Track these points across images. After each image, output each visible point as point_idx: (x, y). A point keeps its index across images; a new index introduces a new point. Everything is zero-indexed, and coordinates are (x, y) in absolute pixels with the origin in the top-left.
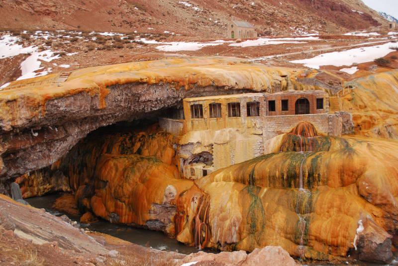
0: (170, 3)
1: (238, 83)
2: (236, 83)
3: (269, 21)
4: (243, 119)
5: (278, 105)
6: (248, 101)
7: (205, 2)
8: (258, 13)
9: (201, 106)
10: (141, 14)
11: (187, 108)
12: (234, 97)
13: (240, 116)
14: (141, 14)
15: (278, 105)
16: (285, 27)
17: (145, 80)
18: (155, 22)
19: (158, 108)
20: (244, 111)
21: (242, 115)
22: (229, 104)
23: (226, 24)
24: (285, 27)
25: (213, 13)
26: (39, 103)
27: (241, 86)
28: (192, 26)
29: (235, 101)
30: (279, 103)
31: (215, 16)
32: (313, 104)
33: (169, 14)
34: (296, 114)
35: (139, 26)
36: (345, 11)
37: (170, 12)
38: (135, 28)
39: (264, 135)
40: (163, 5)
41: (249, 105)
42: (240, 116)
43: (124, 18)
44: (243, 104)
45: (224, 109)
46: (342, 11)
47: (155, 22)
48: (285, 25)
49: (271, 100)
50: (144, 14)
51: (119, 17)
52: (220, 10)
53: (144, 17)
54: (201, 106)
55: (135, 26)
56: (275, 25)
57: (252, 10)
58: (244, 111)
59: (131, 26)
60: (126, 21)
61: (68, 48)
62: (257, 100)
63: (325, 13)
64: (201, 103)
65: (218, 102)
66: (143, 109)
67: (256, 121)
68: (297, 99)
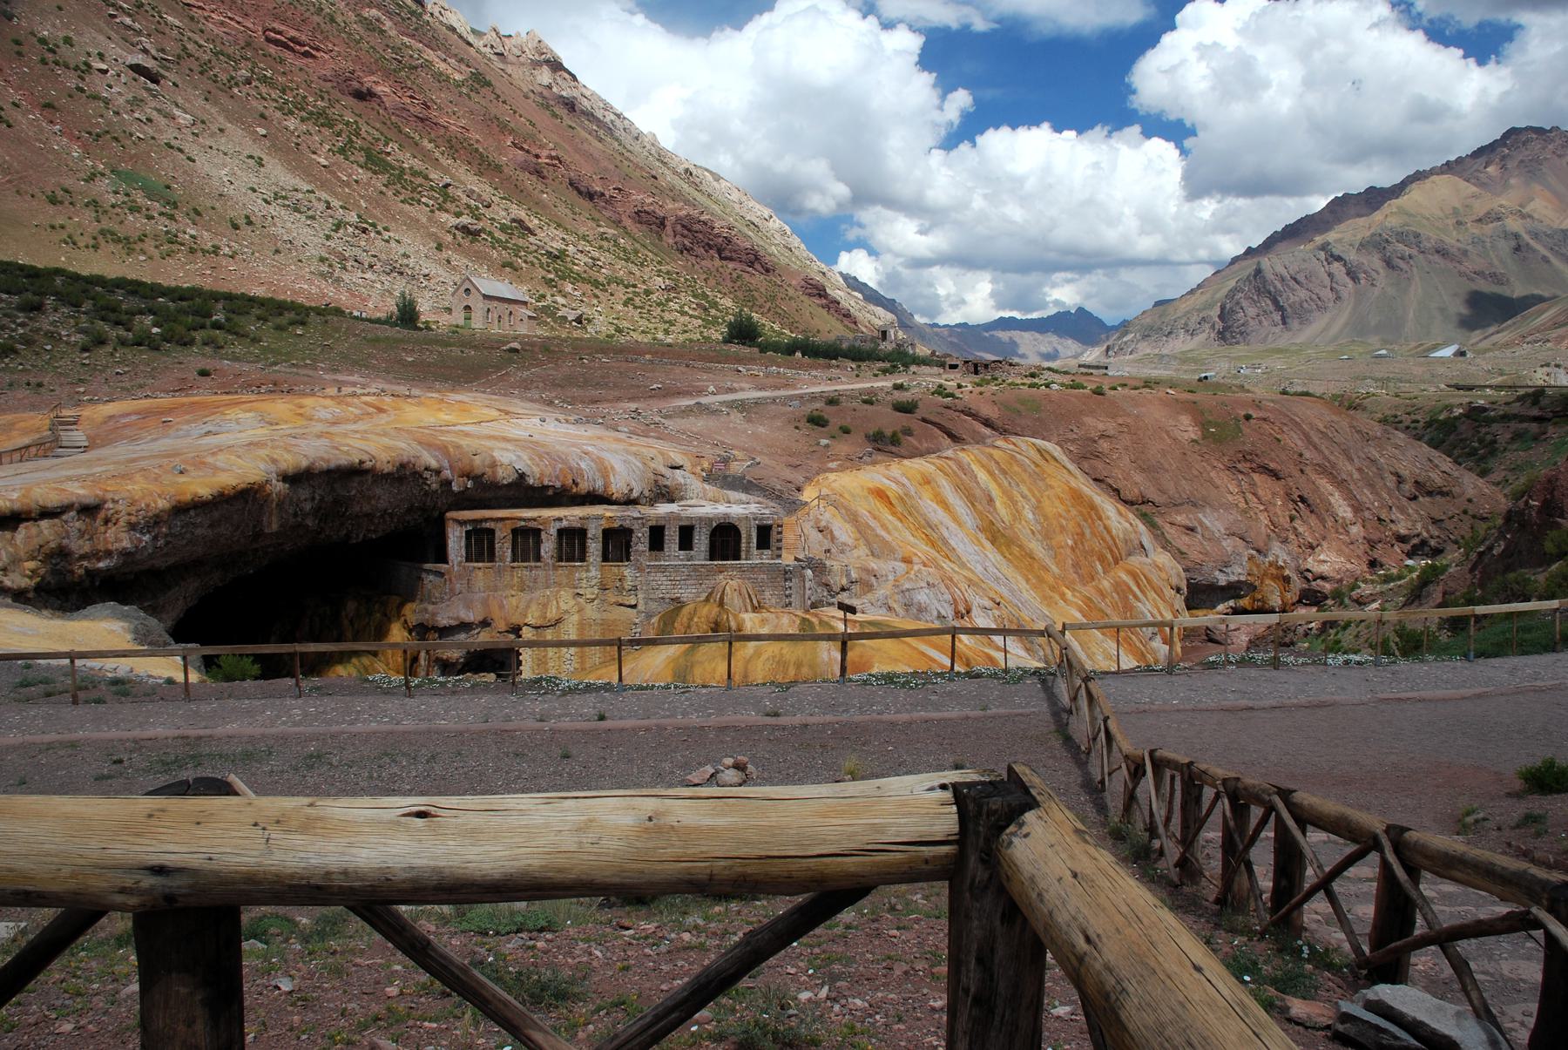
0: (254, 190)
3: (552, 276)
4: (592, 570)
5: (672, 537)
6: (605, 524)
7: (362, 197)
8: (519, 248)
9: (492, 532)
10: (161, 214)
11: (455, 540)
12: (572, 515)
13: (583, 559)
14: (161, 214)
15: (672, 537)
16: (597, 297)
18: (209, 246)
19: (380, 534)
20: (594, 548)
23: (427, 272)
24: (597, 297)
25: (386, 235)
27: (584, 487)
28: (325, 268)
31: (393, 244)
32: (749, 537)
33: (250, 223)
34: (711, 559)
35: (156, 253)
36: (757, 266)
37: (253, 219)
38: (142, 258)
40: (232, 192)
41: (608, 534)
42: (583, 559)
43: (106, 224)
44: (594, 531)
46: (751, 264)
47: (209, 246)
48: (597, 291)
49: (654, 523)
50: (172, 217)
51: (89, 214)
52: (409, 227)
53: (173, 227)
54: (492, 532)
55: (143, 252)
56: (569, 288)
57: (503, 237)
58: (594, 548)
59: (130, 252)
60: (113, 234)
61: (21, 331)
62: (627, 524)
63: (703, 263)
64: (487, 525)
65: (533, 525)
66: (348, 536)
67: (628, 572)
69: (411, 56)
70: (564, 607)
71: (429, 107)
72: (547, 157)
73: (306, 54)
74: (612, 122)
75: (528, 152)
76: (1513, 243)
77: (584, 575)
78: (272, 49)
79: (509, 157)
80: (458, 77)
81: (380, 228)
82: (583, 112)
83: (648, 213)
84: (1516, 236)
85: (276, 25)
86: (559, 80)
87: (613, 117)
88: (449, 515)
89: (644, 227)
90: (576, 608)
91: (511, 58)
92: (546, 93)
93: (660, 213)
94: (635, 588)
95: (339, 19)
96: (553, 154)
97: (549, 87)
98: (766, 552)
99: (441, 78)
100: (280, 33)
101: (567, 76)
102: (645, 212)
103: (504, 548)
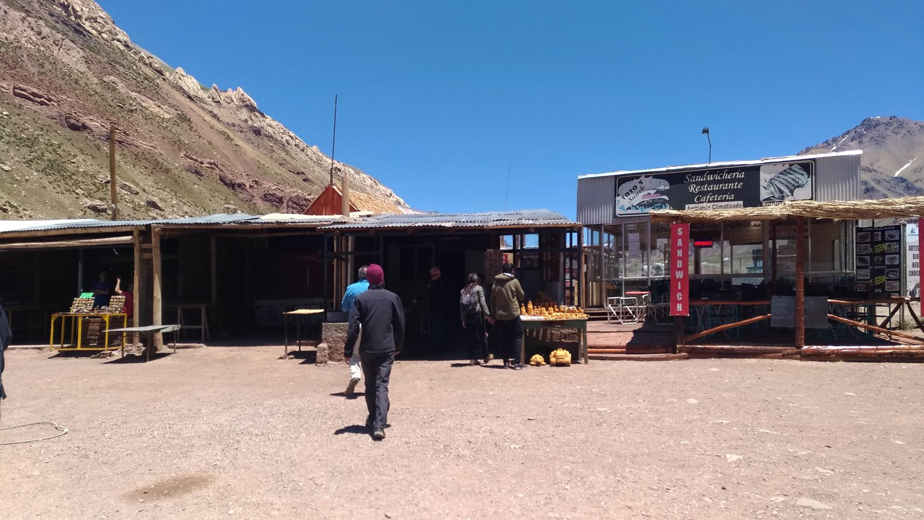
69: (131, 104)
71: (128, 135)
72: (208, 163)
73: (42, 103)
74: (287, 141)
75: (196, 160)
76: (864, 187)
78: (18, 100)
79: (178, 163)
80: (167, 116)
81: (20, 209)
82: (266, 136)
83: (272, 195)
84: (866, 183)
85: (21, 85)
86: (253, 117)
87: (288, 138)
89: (268, 204)
91: (225, 104)
92: (242, 124)
93: (279, 194)
95: (82, 82)
96: (212, 161)
97: (246, 121)
99: (150, 118)
100: (24, 90)
101: (257, 114)
102: (269, 194)
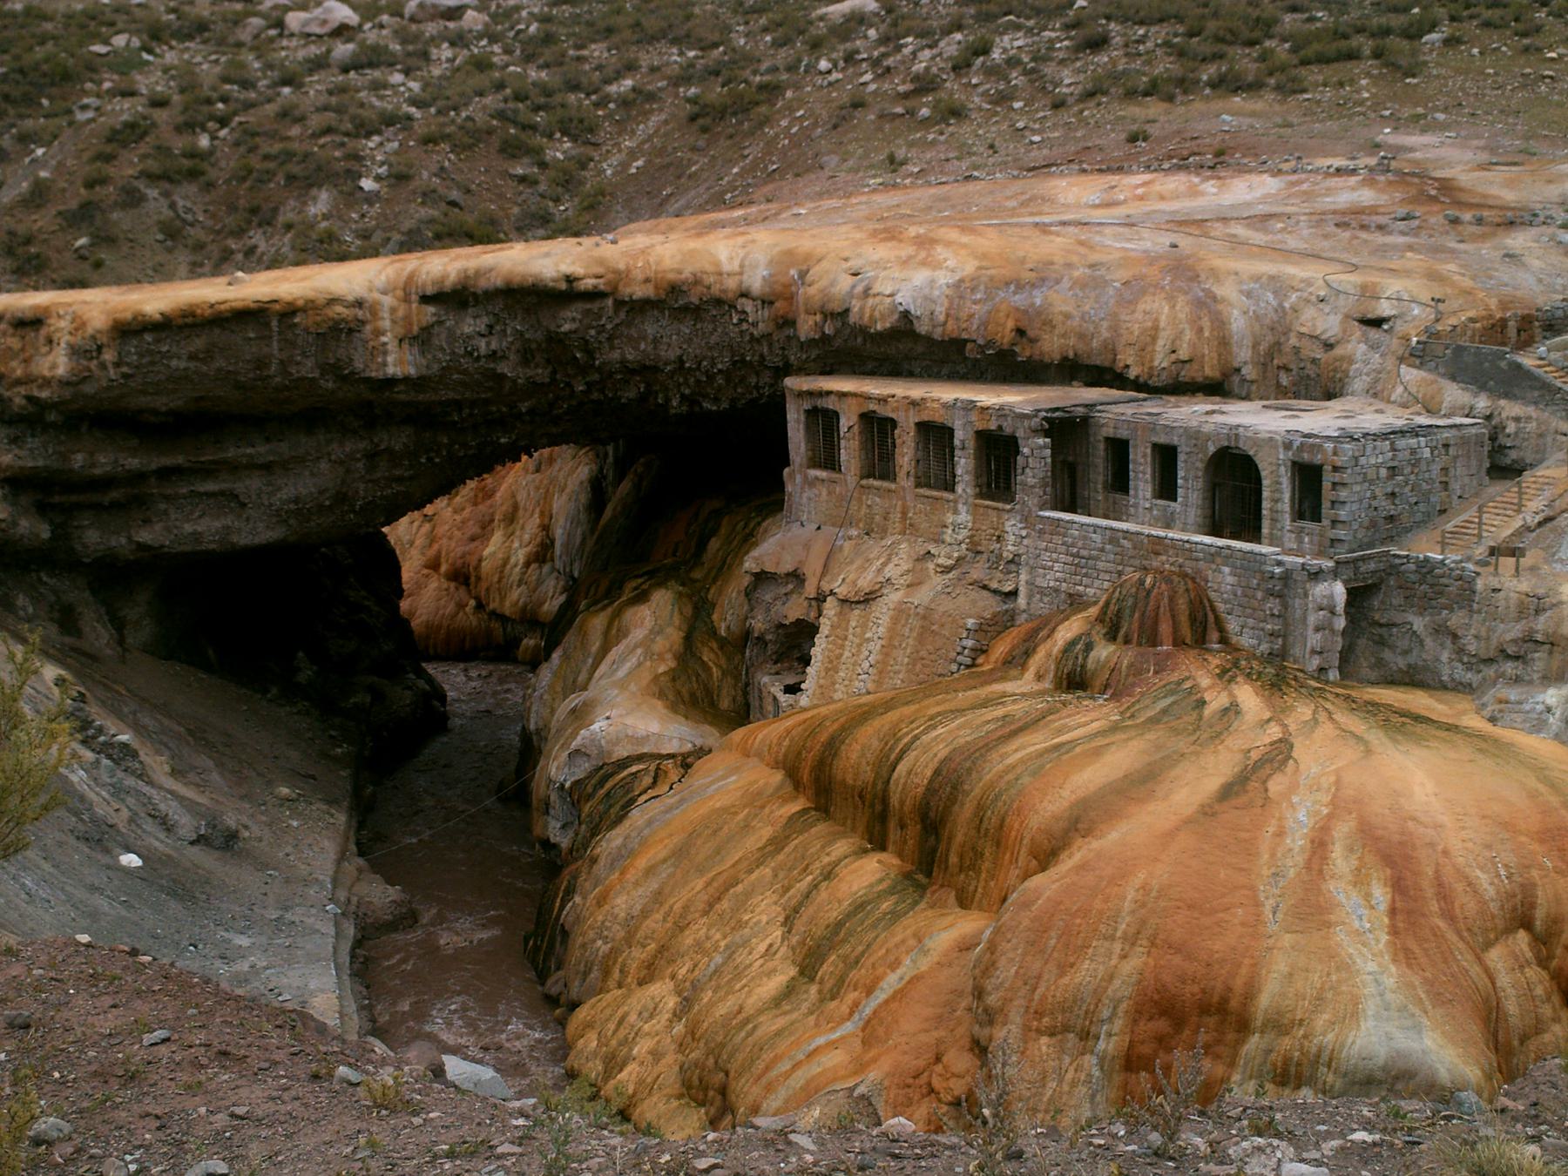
1: (1031, 333)
2: (1020, 332)
17: (589, 283)
19: (725, 405)
21: (959, 489)
22: (925, 428)
26: (93, 337)
27: (1052, 346)
29: (938, 417)
30: (1145, 456)
32: (1277, 492)
39: (1022, 601)
45: (906, 454)
68: (1212, 449)
70: (890, 571)
77: (950, 518)
88: (790, 382)
90: (909, 578)
94: (1014, 561)
98: (1309, 525)
103: (850, 451)
